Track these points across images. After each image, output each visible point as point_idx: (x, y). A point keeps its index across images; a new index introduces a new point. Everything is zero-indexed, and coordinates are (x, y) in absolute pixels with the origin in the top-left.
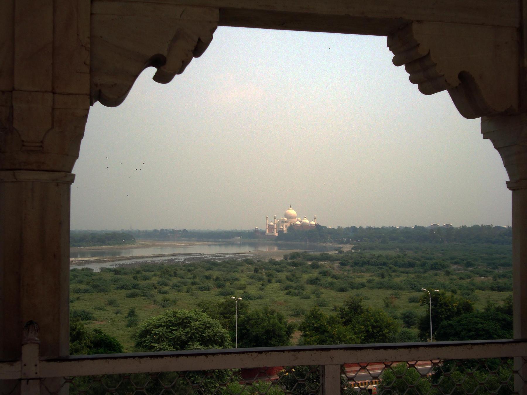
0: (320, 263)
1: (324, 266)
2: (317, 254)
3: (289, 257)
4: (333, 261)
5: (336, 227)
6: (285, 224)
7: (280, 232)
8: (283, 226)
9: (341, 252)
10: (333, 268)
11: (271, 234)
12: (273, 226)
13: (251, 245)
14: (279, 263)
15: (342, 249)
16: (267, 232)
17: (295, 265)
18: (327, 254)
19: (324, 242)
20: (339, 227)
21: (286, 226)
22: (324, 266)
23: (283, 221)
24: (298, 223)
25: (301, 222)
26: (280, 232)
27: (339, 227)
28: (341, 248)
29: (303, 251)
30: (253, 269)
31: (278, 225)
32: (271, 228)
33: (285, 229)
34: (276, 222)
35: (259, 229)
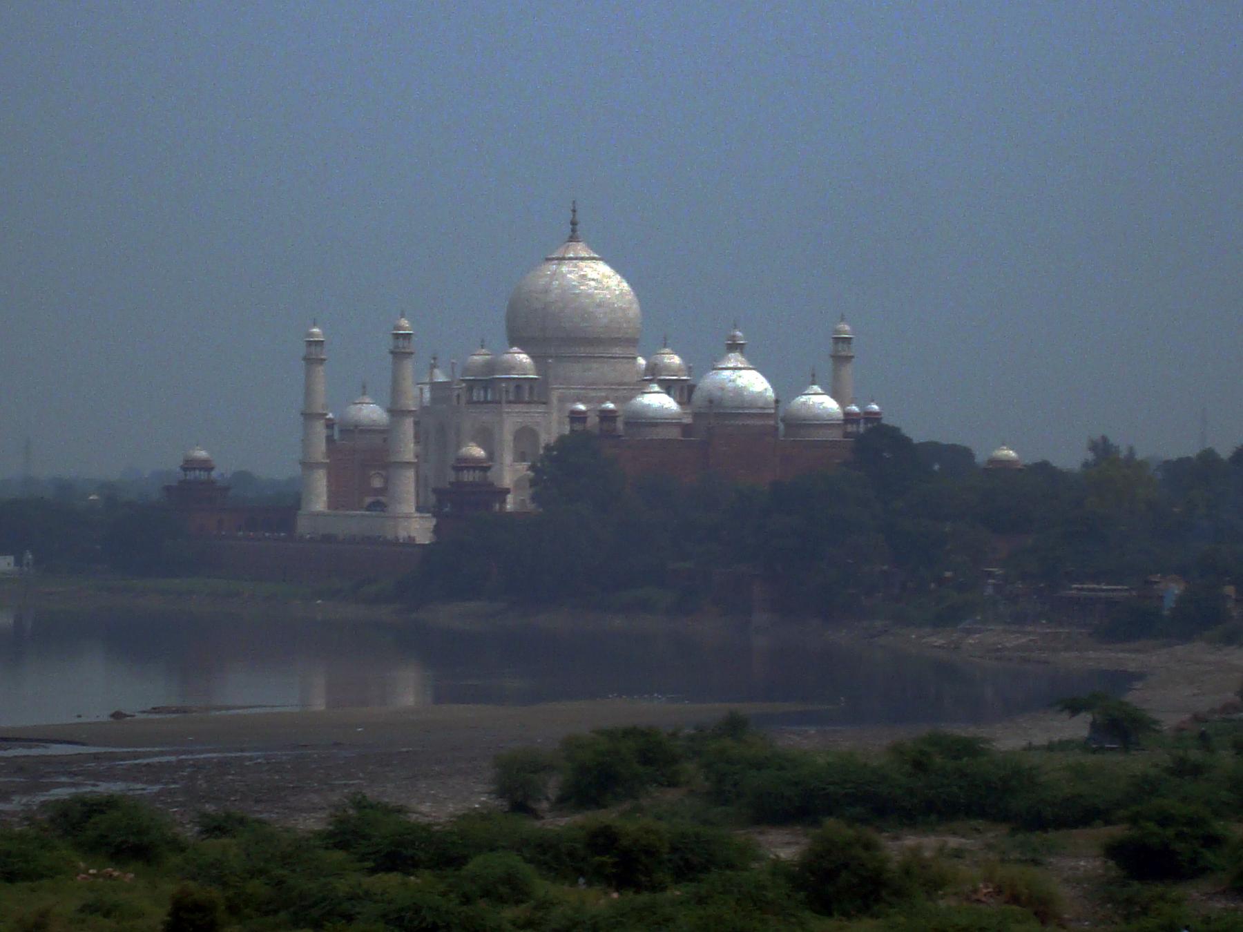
0: (899, 847)
1: (935, 885)
2: (869, 745)
3: (553, 786)
4: (1037, 822)
5: (1070, 457)
6: (511, 420)
7: (463, 499)
8: (486, 438)
9: (1122, 728)
10: (1042, 909)
11: (354, 523)
12: (384, 434)
13: (133, 641)
14: (443, 853)
15: (1134, 697)
16: (319, 502)
17: (622, 863)
18: (969, 748)
19: (946, 618)
20: (1102, 448)
21: (525, 435)
22: (935, 885)
23: (488, 388)
24: (658, 401)
25: (681, 389)
26: (463, 499)
27: (1102, 448)
28: (1125, 679)
29: (713, 711)
30: (160, 914)
31: (437, 426)
32: (359, 459)
33: (510, 472)
34: (416, 395)
35: (224, 469)
